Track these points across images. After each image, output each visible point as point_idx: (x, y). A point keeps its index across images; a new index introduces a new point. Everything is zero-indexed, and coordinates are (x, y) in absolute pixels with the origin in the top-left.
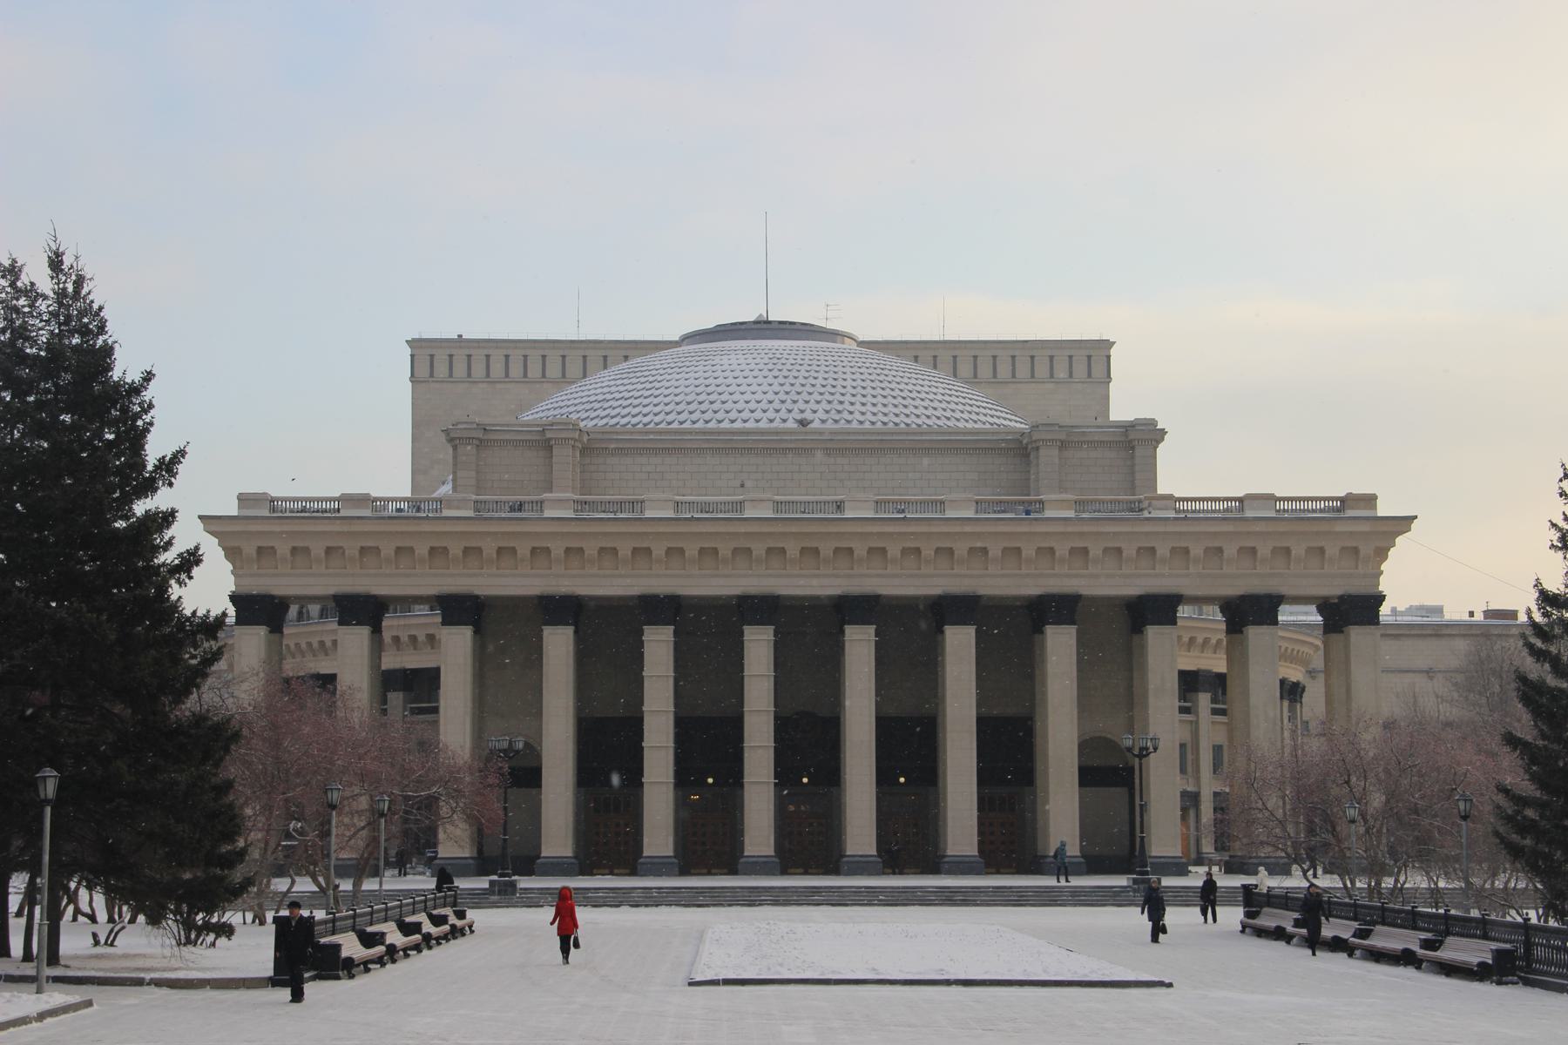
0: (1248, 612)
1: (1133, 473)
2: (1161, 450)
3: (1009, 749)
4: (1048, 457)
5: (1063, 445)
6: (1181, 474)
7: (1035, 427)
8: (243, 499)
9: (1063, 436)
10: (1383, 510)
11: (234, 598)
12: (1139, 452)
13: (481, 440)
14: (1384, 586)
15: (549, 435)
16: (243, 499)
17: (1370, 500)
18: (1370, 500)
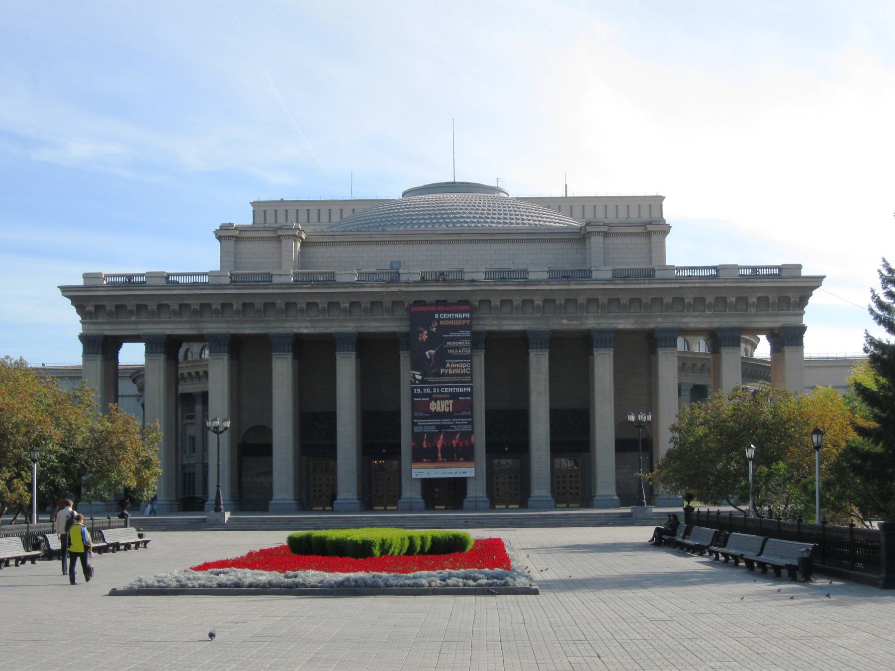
0: (721, 339)
1: (651, 253)
2: (669, 240)
3: (572, 430)
4: (596, 242)
5: (606, 235)
6: (682, 252)
7: (588, 224)
8: (86, 276)
9: (605, 229)
10: (804, 273)
11: (82, 338)
12: (654, 238)
13: (236, 237)
14: (806, 320)
15: (280, 233)
16: (86, 276)
17: (799, 267)
18: (799, 267)
